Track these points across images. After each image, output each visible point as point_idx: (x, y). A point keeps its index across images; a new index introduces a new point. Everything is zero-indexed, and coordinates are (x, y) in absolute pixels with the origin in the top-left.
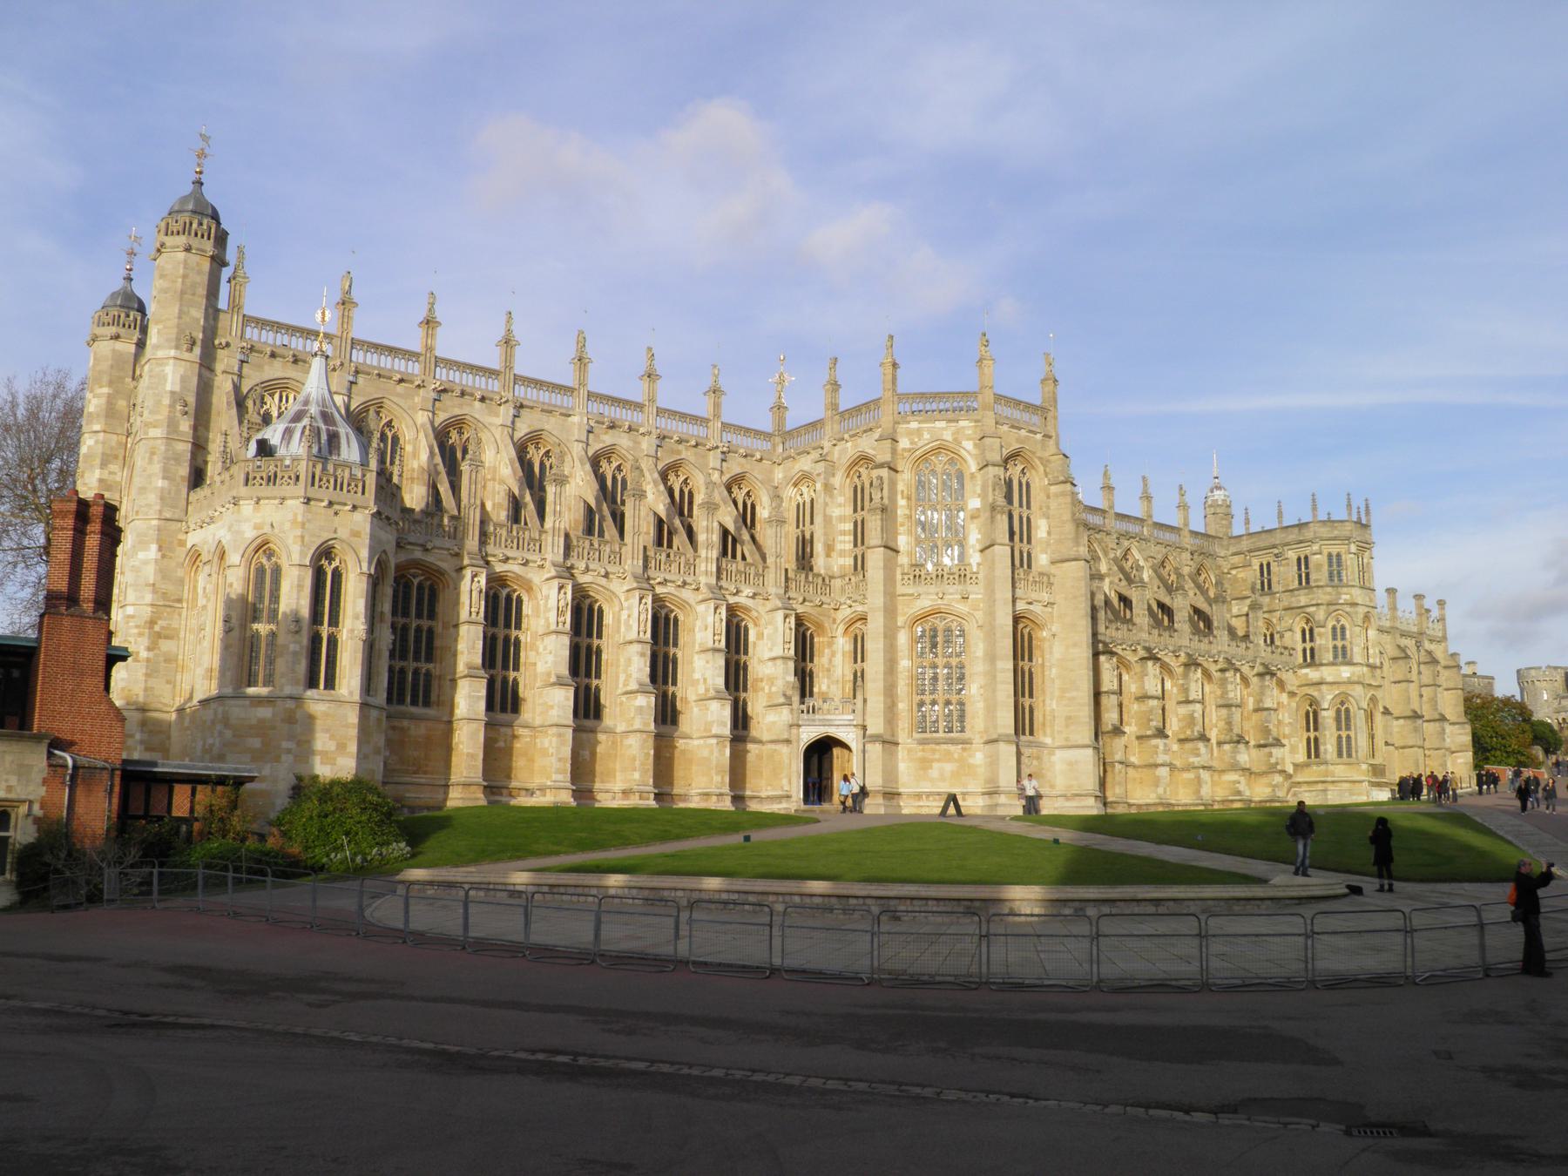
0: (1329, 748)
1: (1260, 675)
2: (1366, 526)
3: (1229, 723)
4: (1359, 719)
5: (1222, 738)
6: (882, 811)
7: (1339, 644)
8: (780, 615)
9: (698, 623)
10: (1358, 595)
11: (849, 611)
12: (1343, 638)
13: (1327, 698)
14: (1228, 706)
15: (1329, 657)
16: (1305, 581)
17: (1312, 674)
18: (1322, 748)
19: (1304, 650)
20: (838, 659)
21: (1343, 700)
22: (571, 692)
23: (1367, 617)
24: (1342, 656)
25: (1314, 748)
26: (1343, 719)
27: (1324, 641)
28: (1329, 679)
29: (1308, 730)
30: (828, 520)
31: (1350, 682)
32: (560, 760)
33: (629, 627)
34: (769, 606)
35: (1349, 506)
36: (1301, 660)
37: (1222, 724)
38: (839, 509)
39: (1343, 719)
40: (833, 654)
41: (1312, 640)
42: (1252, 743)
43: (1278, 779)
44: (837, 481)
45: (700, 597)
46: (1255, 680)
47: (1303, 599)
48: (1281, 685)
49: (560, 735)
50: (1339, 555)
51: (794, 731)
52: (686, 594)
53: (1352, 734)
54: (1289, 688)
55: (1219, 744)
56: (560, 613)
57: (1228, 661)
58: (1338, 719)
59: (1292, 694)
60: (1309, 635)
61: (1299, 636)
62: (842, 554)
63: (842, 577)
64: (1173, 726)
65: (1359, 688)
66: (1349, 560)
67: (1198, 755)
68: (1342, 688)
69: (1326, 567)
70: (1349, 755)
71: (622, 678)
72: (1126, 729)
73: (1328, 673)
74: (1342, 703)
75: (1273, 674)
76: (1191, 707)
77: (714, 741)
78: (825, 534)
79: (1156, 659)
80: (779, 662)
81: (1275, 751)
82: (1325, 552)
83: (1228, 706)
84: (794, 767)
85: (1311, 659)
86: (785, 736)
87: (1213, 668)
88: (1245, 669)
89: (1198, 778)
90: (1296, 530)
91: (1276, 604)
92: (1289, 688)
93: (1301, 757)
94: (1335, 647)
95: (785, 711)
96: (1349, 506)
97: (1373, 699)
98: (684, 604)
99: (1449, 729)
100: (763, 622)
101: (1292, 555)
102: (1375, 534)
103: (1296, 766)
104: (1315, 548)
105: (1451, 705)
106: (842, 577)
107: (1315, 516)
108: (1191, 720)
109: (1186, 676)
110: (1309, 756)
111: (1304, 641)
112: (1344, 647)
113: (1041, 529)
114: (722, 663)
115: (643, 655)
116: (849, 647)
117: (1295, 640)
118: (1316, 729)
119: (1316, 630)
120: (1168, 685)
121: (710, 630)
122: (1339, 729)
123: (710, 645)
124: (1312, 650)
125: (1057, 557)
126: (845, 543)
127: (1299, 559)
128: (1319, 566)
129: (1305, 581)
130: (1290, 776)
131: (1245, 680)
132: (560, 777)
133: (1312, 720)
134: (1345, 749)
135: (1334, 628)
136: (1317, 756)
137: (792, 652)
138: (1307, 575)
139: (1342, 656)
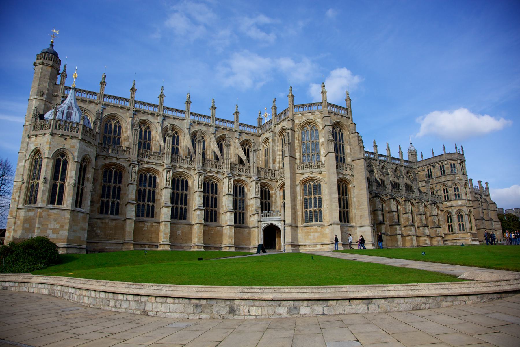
0: (456, 228)
1: (430, 204)
2: (463, 155)
3: (421, 220)
4: (466, 218)
5: (419, 225)
6: (291, 251)
7: (457, 193)
8: (254, 183)
9: (224, 186)
10: (461, 177)
11: (281, 181)
12: (458, 191)
13: (454, 211)
14: (421, 214)
15: (453, 198)
16: (443, 173)
17: (448, 204)
18: (454, 228)
19: (445, 196)
20: (278, 197)
21: (459, 211)
22: (170, 209)
23: (466, 184)
25: (451, 228)
26: (460, 218)
27: (451, 192)
28: (454, 205)
29: (448, 222)
30: (273, 151)
31: (462, 206)
32: (165, 234)
33: (196, 186)
34: (251, 180)
35: (456, 148)
36: (444, 199)
37: (419, 221)
38: (278, 147)
39: (460, 218)
40: (276, 197)
41: (447, 192)
42: (430, 227)
43: (440, 239)
44: (276, 138)
45: (225, 176)
46: (429, 206)
47: (443, 179)
48: (438, 208)
49: (165, 225)
50: (454, 164)
51: (259, 223)
52: (219, 176)
53: (464, 223)
54: (441, 209)
55: (418, 227)
56: (167, 180)
57: (419, 199)
58: (458, 218)
59: (442, 211)
60: (446, 191)
61: (442, 191)
62: (279, 162)
63: (278, 170)
64: (402, 221)
65: (465, 208)
66: (458, 165)
67: (411, 231)
68: (459, 208)
69: (450, 168)
70: (463, 230)
71: (194, 204)
72: (386, 223)
73: (454, 203)
74: (460, 213)
75: (435, 204)
76: (408, 215)
77: (228, 227)
78: (273, 156)
79: (394, 199)
80: (254, 199)
81: (438, 229)
82: (449, 163)
83: (421, 214)
84: (260, 236)
85: (447, 199)
86: (256, 225)
87: (414, 202)
88: (425, 203)
89: (412, 239)
90: (439, 157)
91: (434, 182)
92: (441, 209)
93: (447, 231)
94: (455, 195)
95: (256, 216)
96: (456, 148)
97: (470, 211)
98: (218, 180)
99: (493, 223)
100: (249, 185)
101: (438, 165)
102: (466, 157)
103: (445, 234)
104: (446, 162)
106: (278, 170)
107: (445, 152)
108: (408, 219)
109: (405, 204)
110: (449, 231)
111: (444, 193)
112: (458, 194)
114: (232, 199)
115: (200, 196)
116: (282, 194)
117: (441, 193)
118: (451, 222)
119: (448, 189)
120: (399, 208)
121: (227, 187)
122: (459, 221)
123: (227, 193)
124: (447, 195)
126: (279, 159)
127: (440, 167)
128: (447, 168)
129: (443, 173)
130: (443, 238)
131: (425, 206)
132: (165, 240)
133: (449, 219)
134: (462, 228)
135: (454, 188)
136: (452, 231)
137: (259, 196)
138: (444, 171)
139: (458, 197)
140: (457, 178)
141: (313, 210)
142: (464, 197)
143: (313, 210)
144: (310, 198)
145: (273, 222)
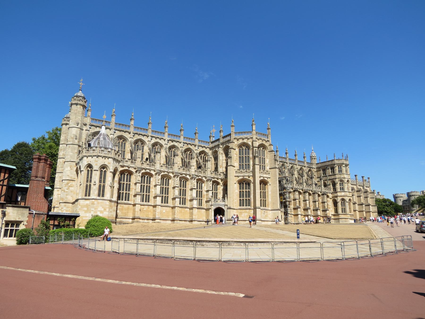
0: (340, 211)
1: (323, 195)
3: (315, 205)
7: (341, 187)
24: (342, 189)
47: (333, 177)
58: (342, 204)
68: (342, 197)
94: (340, 188)
105: (371, 201)
113: (267, 161)
122: (342, 206)
125: (271, 167)
133: (335, 203)
134: (344, 210)
135: (340, 183)
140: (342, 176)
141: (245, 198)
142: (346, 190)
143: (245, 198)
144: (243, 191)
145: (220, 206)
